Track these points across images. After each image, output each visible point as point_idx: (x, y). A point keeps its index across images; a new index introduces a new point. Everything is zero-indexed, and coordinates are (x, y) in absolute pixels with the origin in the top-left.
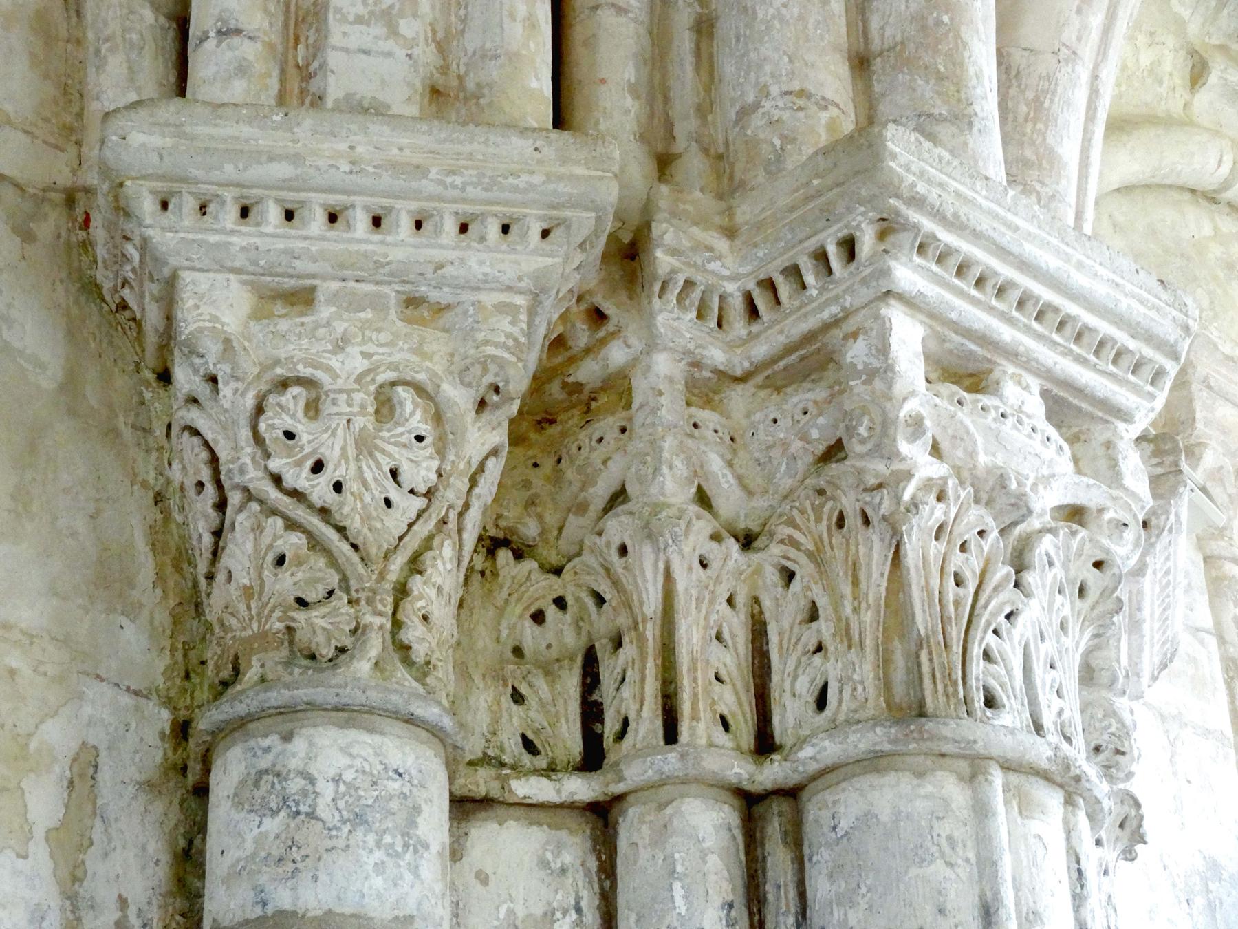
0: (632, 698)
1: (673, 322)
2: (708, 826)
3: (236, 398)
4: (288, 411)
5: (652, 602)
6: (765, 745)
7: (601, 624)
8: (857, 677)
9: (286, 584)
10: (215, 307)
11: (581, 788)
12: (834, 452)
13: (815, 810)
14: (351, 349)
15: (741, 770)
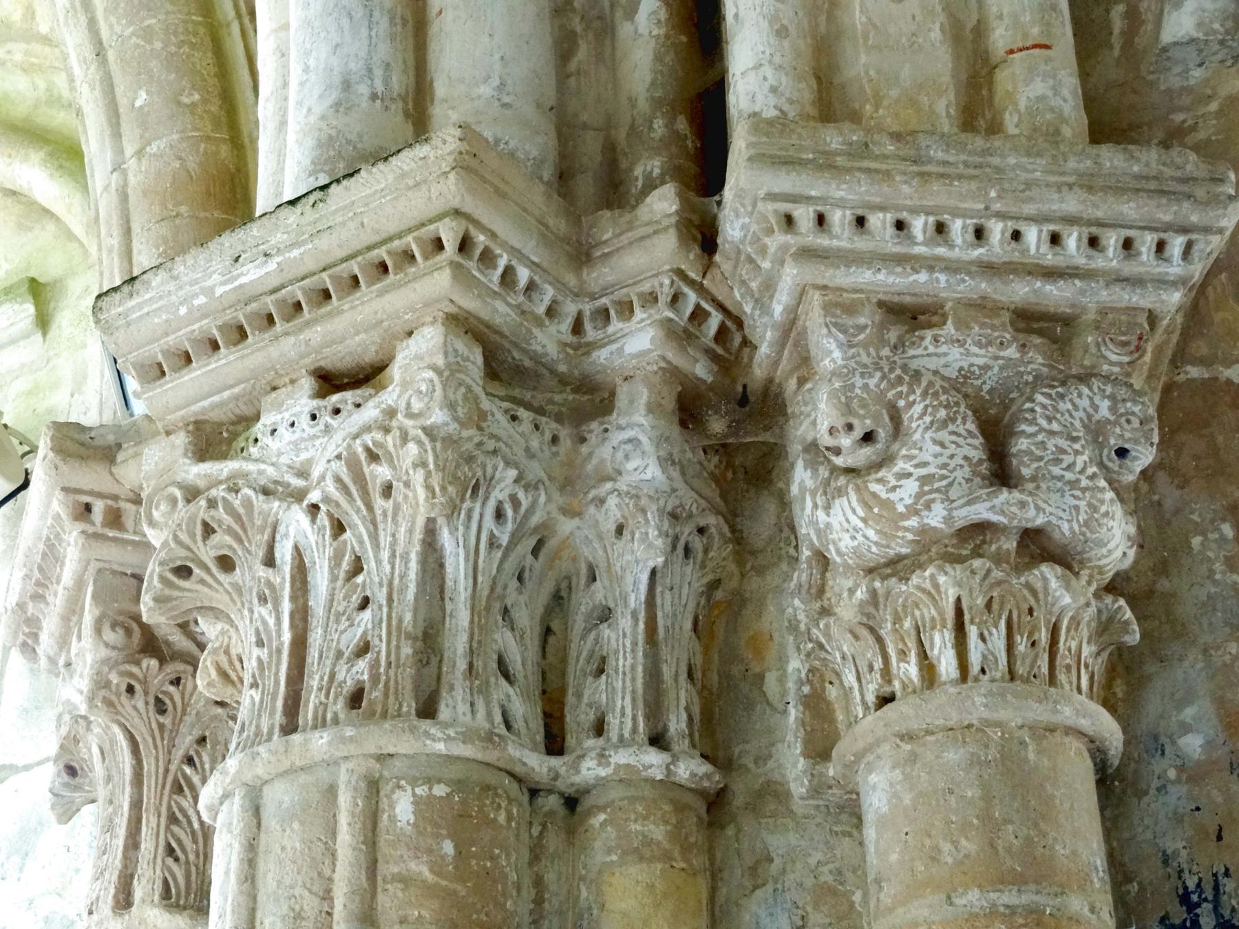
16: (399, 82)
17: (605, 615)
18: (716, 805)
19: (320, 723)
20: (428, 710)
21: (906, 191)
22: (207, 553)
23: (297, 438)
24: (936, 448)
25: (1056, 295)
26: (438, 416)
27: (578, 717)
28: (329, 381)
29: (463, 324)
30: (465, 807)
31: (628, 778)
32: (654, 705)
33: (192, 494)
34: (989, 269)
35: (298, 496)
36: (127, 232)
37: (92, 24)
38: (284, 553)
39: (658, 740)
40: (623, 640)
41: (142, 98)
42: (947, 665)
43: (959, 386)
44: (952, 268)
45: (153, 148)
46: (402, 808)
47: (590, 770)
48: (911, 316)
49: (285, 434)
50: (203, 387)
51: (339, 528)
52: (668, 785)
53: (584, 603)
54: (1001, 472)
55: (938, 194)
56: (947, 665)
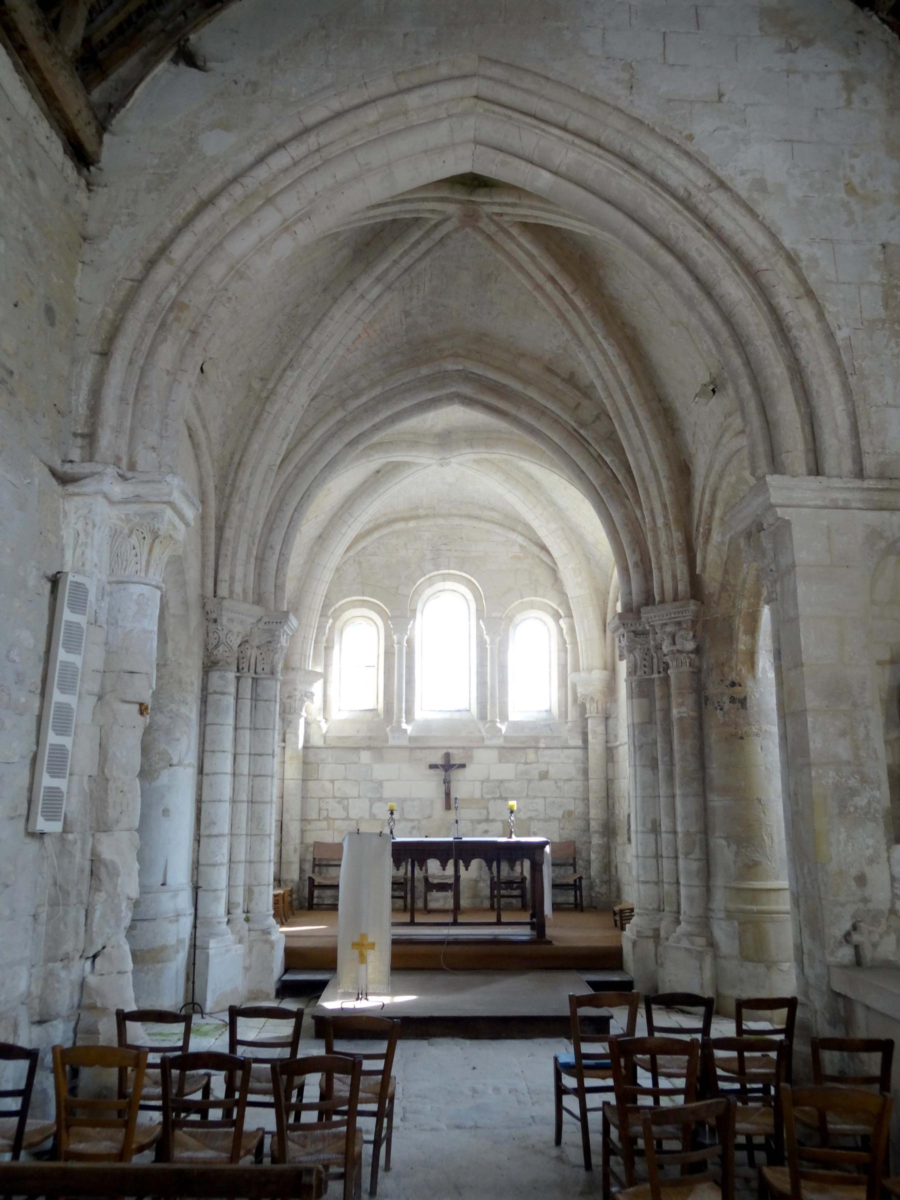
0: (245, 665)
1: (261, 625)
2: (250, 680)
3: (225, 632)
4: (229, 635)
5: (249, 654)
6: (255, 673)
7: (241, 655)
8: (268, 669)
9: (226, 654)
10: (225, 620)
11: (238, 674)
12: (270, 642)
13: (259, 681)
14: (237, 628)
15: (254, 676)
25: (678, 619)
30: (640, 683)
32: (658, 668)
43: (669, 633)
48: (666, 624)
52: (660, 678)
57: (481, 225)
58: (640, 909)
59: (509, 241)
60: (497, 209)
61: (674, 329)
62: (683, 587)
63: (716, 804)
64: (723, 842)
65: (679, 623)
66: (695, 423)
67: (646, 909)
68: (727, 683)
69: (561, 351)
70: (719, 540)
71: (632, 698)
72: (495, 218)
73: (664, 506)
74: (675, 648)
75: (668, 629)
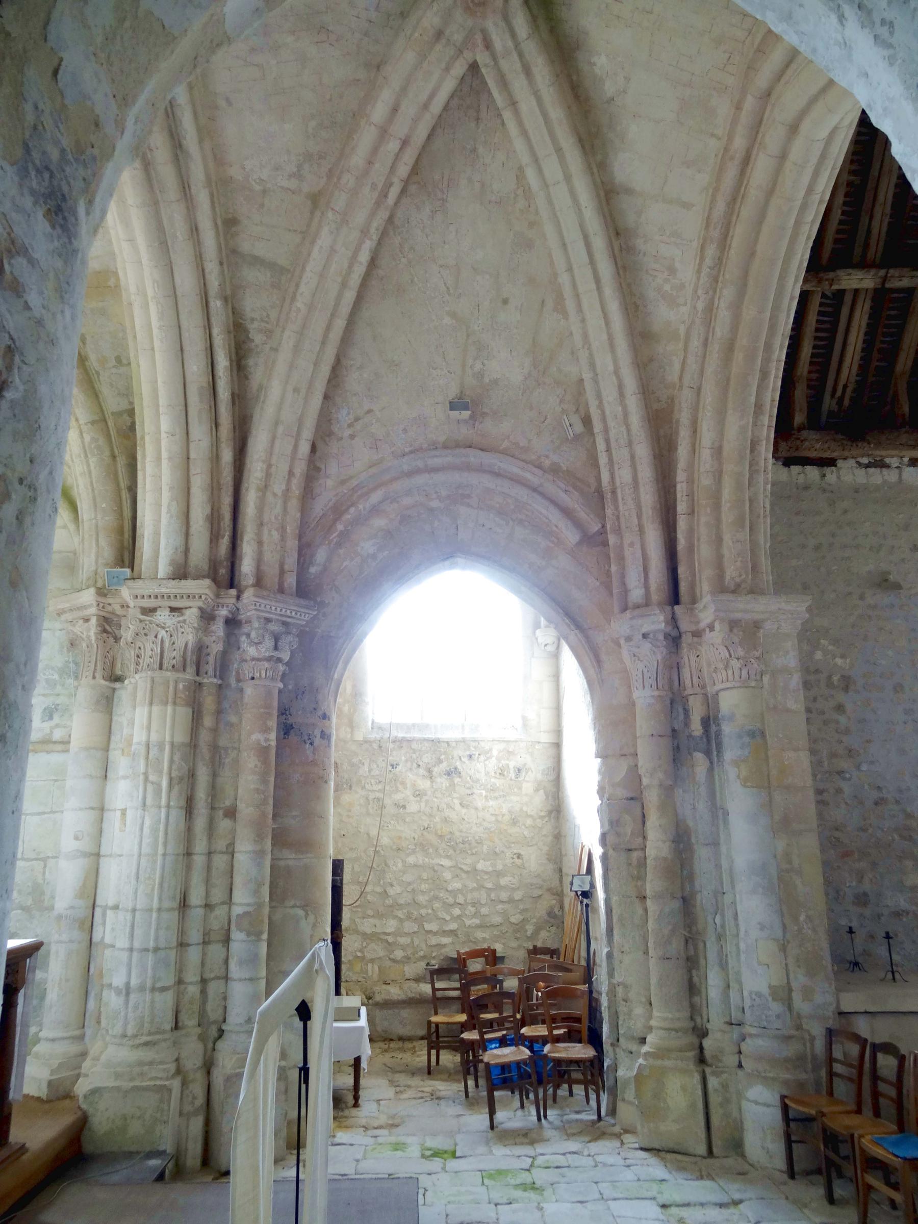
16: (182, 549)
17: (209, 654)
18: (220, 687)
19: (167, 670)
20: (184, 670)
21: (273, 603)
22: (143, 632)
23: (163, 616)
24: (269, 643)
25: (289, 620)
26: (196, 625)
27: (202, 670)
28: (173, 610)
29: (200, 608)
31: (211, 683)
33: (141, 621)
34: (281, 615)
35: (164, 628)
36: (98, 535)
37: (92, 483)
38: (159, 637)
39: (215, 676)
40: (211, 659)
41: (104, 505)
42: (263, 675)
44: (276, 614)
45: (107, 518)
46: (181, 686)
47: (205, 680)
48: (268, 620)
49: (162, 617)
50: (147, 603)
51: (171, 636)
53: (205, 651)
54: (276, 648)
55: (277, 604)
56: (263, 675)
57: (459, 16)
58: (150, 1034)
59: (443, 65)
60: (500, 41)
61: (447, 320)
62: (291, 580)
63: (290, 863)
64: (301, 912)
65: (284, 624)
66: (370, 411)
67: (164, 1032)
68: (320, 713)
69: (257, 188)
70: (371, 551)
71: (175, 703)
72: (479, 38)
73: (291, 473)
74: (276, 654)
75: (273, 627)
